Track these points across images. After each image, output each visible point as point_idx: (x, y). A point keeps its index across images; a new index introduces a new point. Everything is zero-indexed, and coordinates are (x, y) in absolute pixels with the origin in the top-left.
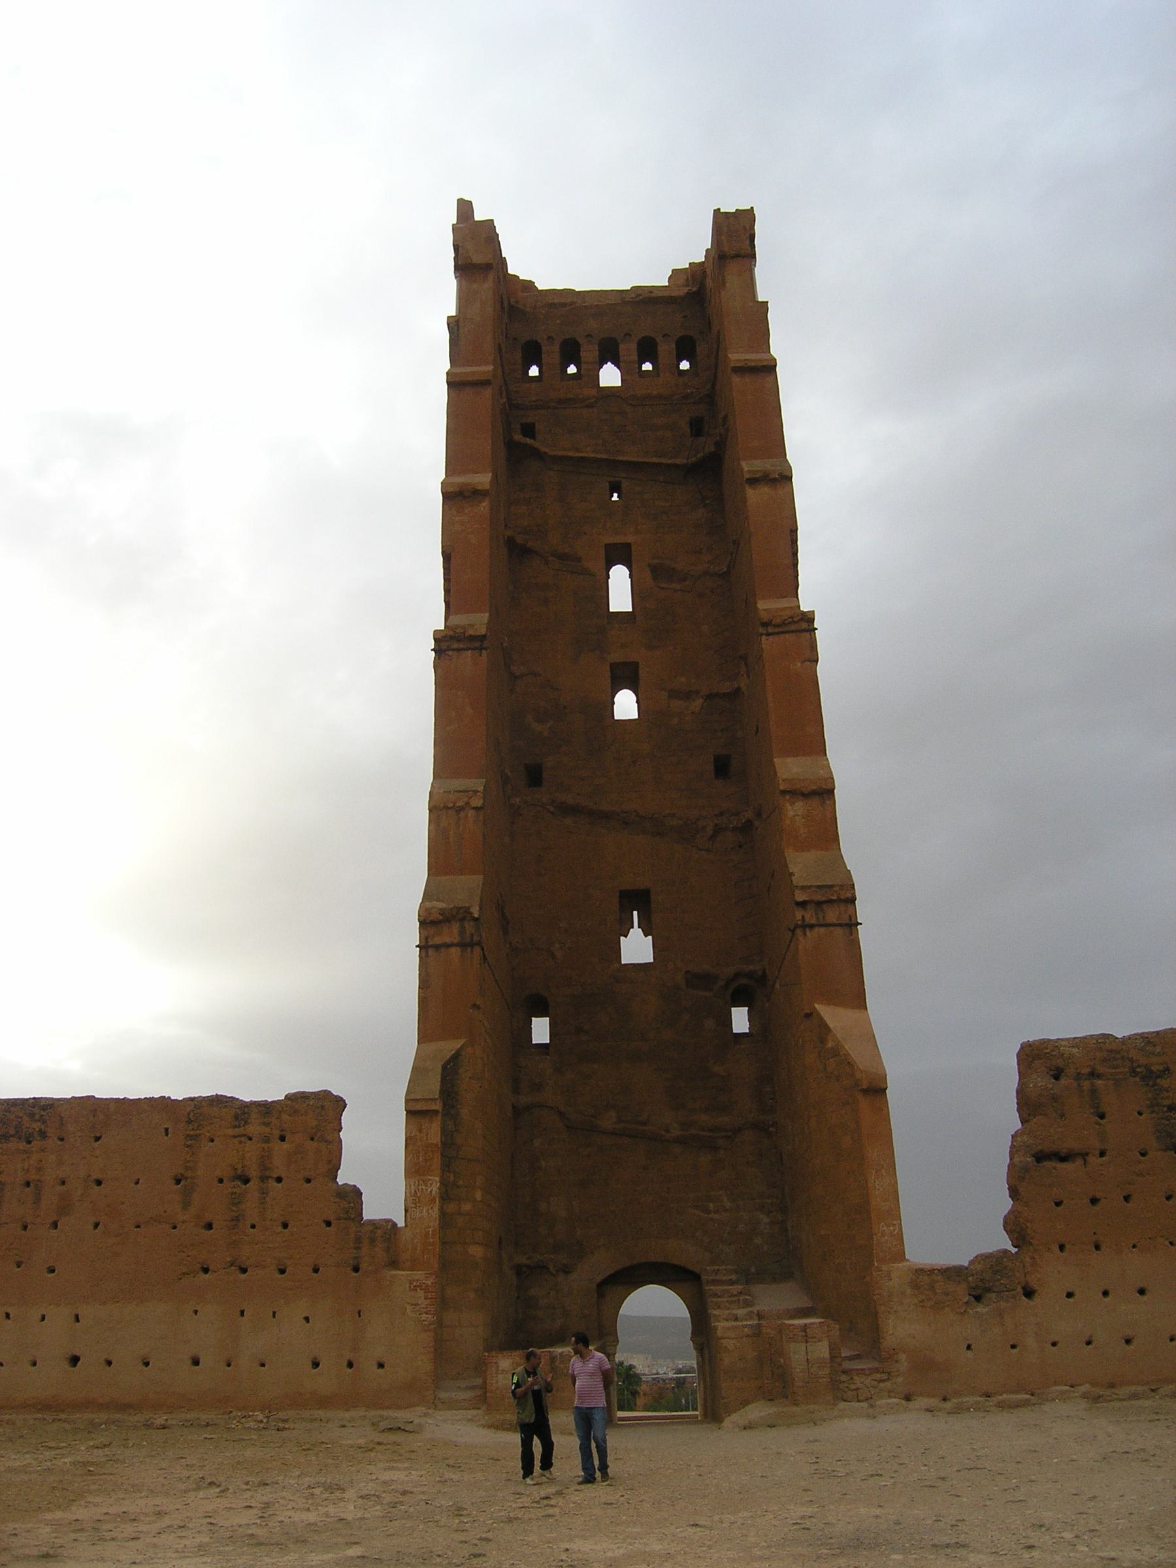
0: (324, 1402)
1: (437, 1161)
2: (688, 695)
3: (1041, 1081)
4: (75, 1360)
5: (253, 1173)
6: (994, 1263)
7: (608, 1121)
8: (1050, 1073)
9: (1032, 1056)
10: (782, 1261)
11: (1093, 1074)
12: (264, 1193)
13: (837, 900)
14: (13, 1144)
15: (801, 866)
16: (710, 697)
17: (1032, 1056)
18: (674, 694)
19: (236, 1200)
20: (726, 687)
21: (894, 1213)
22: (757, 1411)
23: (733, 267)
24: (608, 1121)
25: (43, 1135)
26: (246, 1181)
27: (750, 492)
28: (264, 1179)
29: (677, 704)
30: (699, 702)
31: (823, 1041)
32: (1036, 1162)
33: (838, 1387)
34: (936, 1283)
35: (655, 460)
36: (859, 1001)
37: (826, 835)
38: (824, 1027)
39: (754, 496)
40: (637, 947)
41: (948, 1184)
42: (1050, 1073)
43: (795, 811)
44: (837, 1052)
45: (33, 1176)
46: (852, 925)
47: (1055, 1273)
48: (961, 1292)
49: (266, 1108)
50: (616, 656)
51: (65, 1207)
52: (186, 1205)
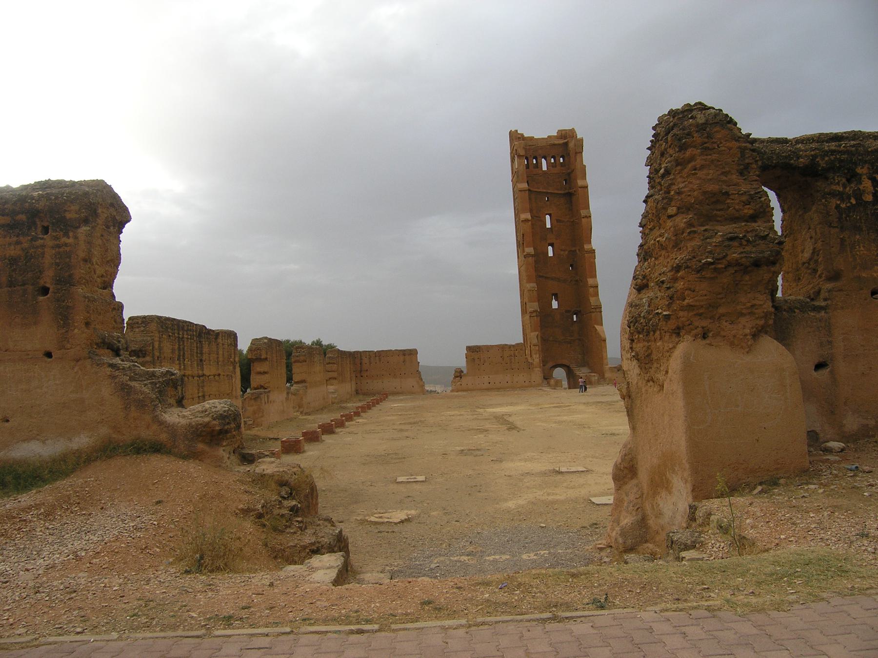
7: (551, 339)
10: (584, 364)
15: (592, 300)
20: (573, 249)
24: (551, 339)
29: (562, 253)
33: (598, 383)
37: (597, 294)
40: (555, 304)
43: (591, 290)
49: (513, 346)
50: (549, 241)
51: (485, 361)
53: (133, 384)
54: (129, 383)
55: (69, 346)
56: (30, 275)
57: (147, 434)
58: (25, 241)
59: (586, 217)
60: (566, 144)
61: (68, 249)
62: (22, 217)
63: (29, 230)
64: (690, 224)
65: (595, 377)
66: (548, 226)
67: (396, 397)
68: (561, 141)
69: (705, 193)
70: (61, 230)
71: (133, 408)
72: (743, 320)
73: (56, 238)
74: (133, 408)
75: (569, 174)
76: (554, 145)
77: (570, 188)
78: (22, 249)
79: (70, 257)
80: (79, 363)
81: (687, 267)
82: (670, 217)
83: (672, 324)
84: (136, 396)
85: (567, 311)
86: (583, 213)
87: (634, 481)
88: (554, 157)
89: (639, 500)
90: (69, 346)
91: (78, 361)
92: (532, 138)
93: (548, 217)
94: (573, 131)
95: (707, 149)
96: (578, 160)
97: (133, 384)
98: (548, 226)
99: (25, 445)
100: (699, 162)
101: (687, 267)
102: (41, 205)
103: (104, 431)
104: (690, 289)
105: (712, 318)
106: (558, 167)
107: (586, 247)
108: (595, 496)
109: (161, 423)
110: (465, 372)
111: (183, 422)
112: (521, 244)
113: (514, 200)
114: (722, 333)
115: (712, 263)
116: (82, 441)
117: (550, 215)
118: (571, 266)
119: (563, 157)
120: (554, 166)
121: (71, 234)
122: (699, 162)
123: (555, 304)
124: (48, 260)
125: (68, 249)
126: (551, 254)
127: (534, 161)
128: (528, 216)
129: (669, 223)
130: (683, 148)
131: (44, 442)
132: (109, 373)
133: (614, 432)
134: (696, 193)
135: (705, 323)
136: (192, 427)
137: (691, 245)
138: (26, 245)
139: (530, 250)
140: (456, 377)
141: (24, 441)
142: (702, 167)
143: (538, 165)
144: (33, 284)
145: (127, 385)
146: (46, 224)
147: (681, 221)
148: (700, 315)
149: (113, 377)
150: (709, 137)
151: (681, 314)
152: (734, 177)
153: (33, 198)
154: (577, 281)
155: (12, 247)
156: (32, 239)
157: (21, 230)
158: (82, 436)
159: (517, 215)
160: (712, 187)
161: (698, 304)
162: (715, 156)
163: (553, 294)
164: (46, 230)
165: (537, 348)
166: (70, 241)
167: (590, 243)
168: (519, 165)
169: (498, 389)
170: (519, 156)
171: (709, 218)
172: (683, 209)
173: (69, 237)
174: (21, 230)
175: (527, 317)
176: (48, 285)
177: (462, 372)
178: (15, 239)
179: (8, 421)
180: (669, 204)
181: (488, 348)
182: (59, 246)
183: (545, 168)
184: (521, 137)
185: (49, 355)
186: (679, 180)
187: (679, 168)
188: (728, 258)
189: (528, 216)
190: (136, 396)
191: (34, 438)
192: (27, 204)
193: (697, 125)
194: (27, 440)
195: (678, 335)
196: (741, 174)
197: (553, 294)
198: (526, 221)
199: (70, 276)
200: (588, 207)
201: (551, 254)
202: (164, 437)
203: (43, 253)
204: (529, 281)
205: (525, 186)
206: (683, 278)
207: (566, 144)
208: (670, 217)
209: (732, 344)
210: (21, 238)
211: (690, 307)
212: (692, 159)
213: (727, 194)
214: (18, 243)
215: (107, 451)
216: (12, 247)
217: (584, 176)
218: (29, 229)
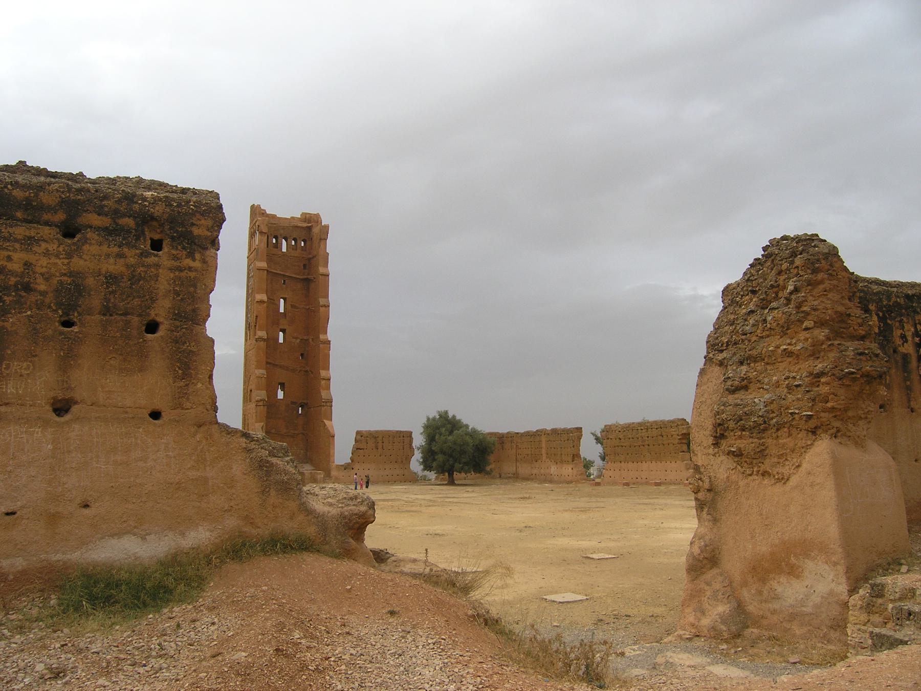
2: (296, 338)
3: (359, 437)
6: (348, 464)
8: (361, 437)
9: (358, 433)
13: (330, 402)
15: (324, 394)
17: (358, 433)
23: (322, 242)
29: (294, 340)
30: (298, 341)
32: (357, 450)
34: (339, 467)
37: (328, 388)
39: (322, 309)
40: (280, 395)
41: (342, 451)
42: (361, 437)
43: (323, 382)
47: (357, 466)
50: (282, 327)
53: (274, 460)
54: (269, 459)
55: (188, 405)
56: (136, 302)
57: (290, 526)
58: (131, 255)
59: (325, 306)
60: (309, 229)
61: (192, 275)
62: (130, 222)
63: (136, 240)
64: (828, 339)
65: (320, 475)
66: (282, 310)
68: (305, 225)
69: (836, 312)
70: (184, 248)
71: (273, 493)
72: (861, 423)
73: (175, 258)
74: (273, 493)
75: (309, 259)
78: (127, 266)
79: (195, 286)
80: (202, 429)
81: (834, 375)
82: (807, 329)
83: (812, 424)
84: (278, 477)
85: (293, 403)
86: (322, 301)
87: (715, 571)
88: (295, 239)
89: (728, 589)
90: (188, 405)
91: (200, 426)
92: (274, 216)
93: (282, 301)
94: (318, 216)
95: (831, 275)
97: (274, 460)
98: (282, 310)
99: (114, 541)
100: (827, 284)
101: (834, 375)
102: (158, 210)
103: (232, 523)
104: (833, 394)
105: (842, 420)
106: (299, 251)
107: (322, 337)
108: (552, 593)
109: (309, 512)
111: (334, 511)
112: (250, 327)
113: (248, 278)
114: (848, 434)
115: (853, 373)
116: (200, 536)
117: (285, 299)
118: (302, 355)
119: (305, 241)
120: (295, 248)
121: (197, 256)
122: (827, 284)
123: (280, 395)
124: (163, 284)
125: (192, 275)
126: (281, 340)
127: (274, 241)
128: (264, 297)
129: (803, 335)
130: (815, 271)
131: (144, 538)
132: (244, 445)
133: (438, 532)
134: (829, 312)
135: (837, 424)
136: (345, 517)
137: (832, 355)
138: (132, 261)
139: (262, 334)
141: (112, 536)
142: (830, 290)
143: (278, 246)
144: (140, 315)
145: (268, 462)
146: (157, 237)
147: (821, 334)
148: (835, 417)
149: (249, 451)
150: (831, 265)
151: (823, 414)
152: (847, 301)
153: (144, 199)
154: (307, 371)
155: (112, 260)
156: (141, 254)
157: (124, 239)
158: (200, 528)
159: (249, 295)
160: (840, 309)
161: (839, 407)
162: (835, 282)
163: (280, 384)
164: (157, 245)
166: (197, 264)
168: (260, 241)
170: (261, 233)
171: (837, 334)
172: (820, 324)
173: (194, 260)
174: (124, 239)
175: (253, 405)
176: (159, 319)
178: (116, 250)
179: (86, 506)
180: (805, 318)
182: (180, 269)
183: (284, 249)
184: (263, 213)
185: (155, 415)
186: (811, 298)
187: (810, 287)
188: (863, 370)
189: (264, 297)
190: (278, 477)
191: (128, 532)
192: (137, 206)
193: (824, 254)
194: (119, 534)
195: (814, 433)
196: (850, 299)
197: (280, 384)
198: (262, 302)
199: (194, 311)
200: (327, 296)
201: (281, 340)
202: (311, 530)
203: (157, 276)
204: (258, 367)
205: (264, 265)
206: (828, 384)
208: (807, 329)
209: (856, 444)
210: (126, 250)
211: (833, 409)
212: (822, 282)
213: (849, 315)
214: (120, 256)
215: (236, 550)
216: (112, 260)
217: (326, 264)
218: (138, 239)
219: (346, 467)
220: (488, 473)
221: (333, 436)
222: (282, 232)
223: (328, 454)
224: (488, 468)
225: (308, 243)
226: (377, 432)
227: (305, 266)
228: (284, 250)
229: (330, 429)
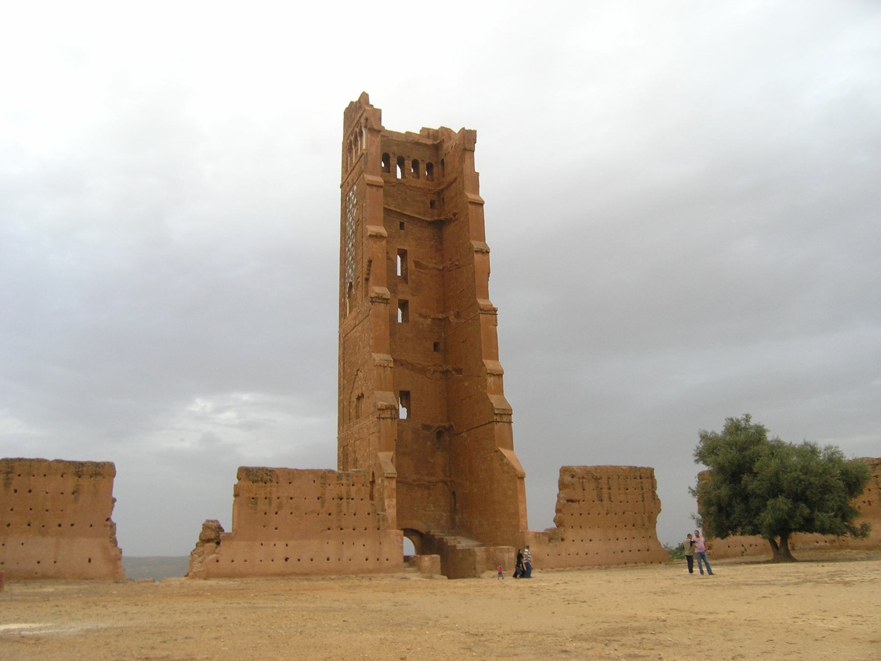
0: (370, 571)
1: (395, 494)
2: (425, 317)
3: (567, 479)
4: (286, 559)
5: (344, 496)
6: (553, 531)
9: (564, 470)
11: (583, 478)
12: (348, 503)
13: (507, 413)
14: (260, 484)
16: (433, 319)
17: (564, 470)
18: (421, 315)
19: (339, 506)
20: (440, 316)
21: (525, 515)
22: (488, 574)
23: (468, 154)
25: (271, 481)
26: (341, 499)
27: (475, 255)
28: (348, 499)
29: (421, 320)
30: (429, 321)
31: (502, 460)
34: (537, 535)
35: (418, 216)
36: (511, 448)
37: (500, 390)
38: (502, 457)
41: (539, 507)
43: (491, 380)
44: (508, 464)
45: (268, 496)
46: (510, 422)
47: (570, 534)
48: (547, 539)
50: (400, 297)
51: (280, 507)
52: (322, 507)
60: (437, 147)
66: (399, 274)
67: (31, 589)
68: (430, 142)
75: (440, 193)
76: (418, 144)
77: (439, 216)
96: (467, 161)
98: (399, 274)
110: (228, 528)
117: (403, 254)
126: (400, 320)
140: (204, 540)
165: (394, 484)
167: (486, 297)
169: (306, 575)
177: (220, 529)
181: (291, 475)
198: (377, 237)
200: (482, 237)
207: (437, 147)
219: (550, 537)
220: (854, 532)
221: (522, 478)
222: (395, 148)
223: (516, 515)
224: (857, 523)
225: (435, 170)
226: (597, 468)
227: (432, 204)
228: (399, 176)
229: (513, 463)
